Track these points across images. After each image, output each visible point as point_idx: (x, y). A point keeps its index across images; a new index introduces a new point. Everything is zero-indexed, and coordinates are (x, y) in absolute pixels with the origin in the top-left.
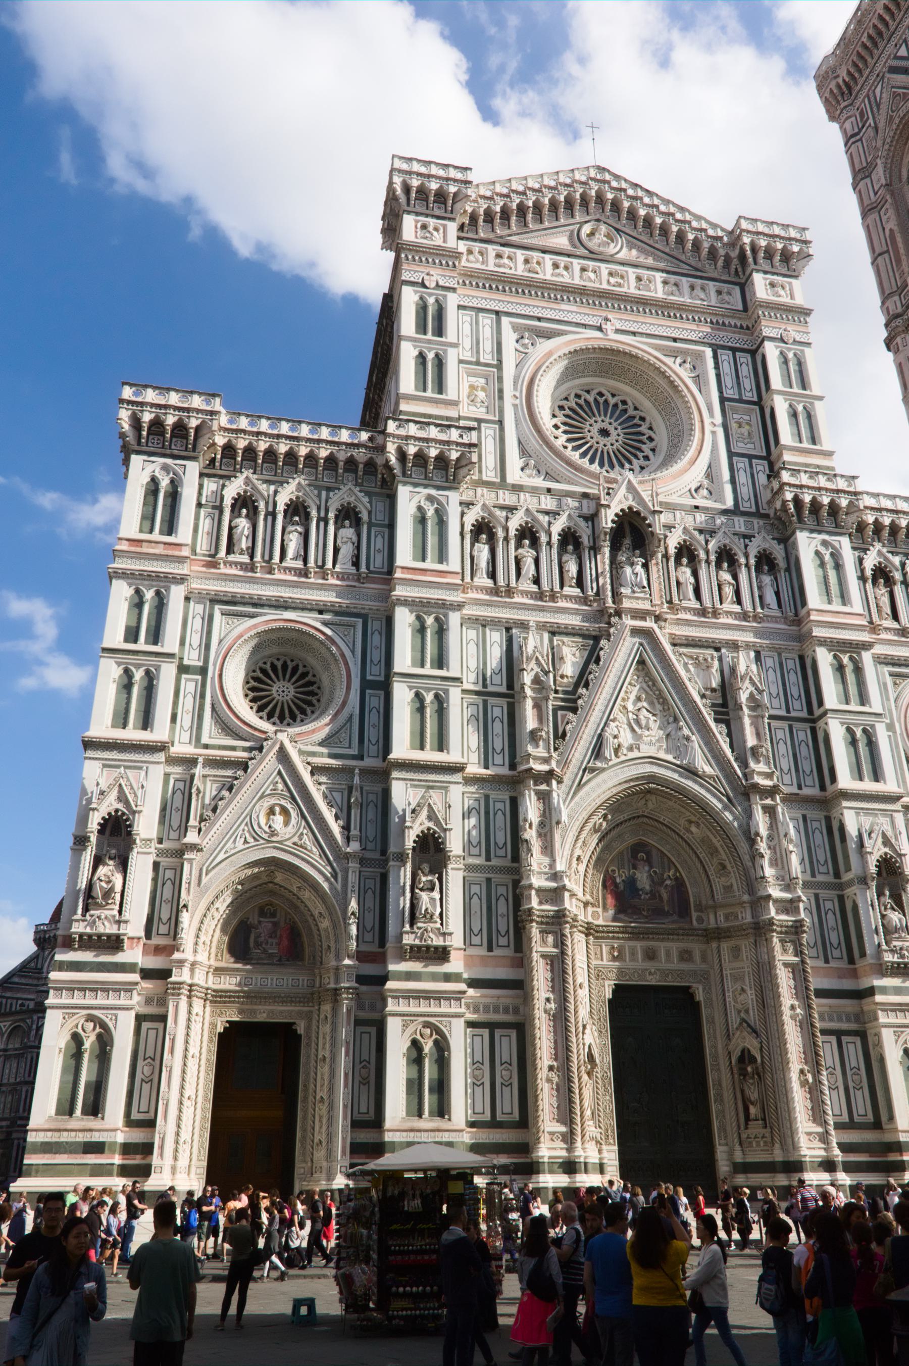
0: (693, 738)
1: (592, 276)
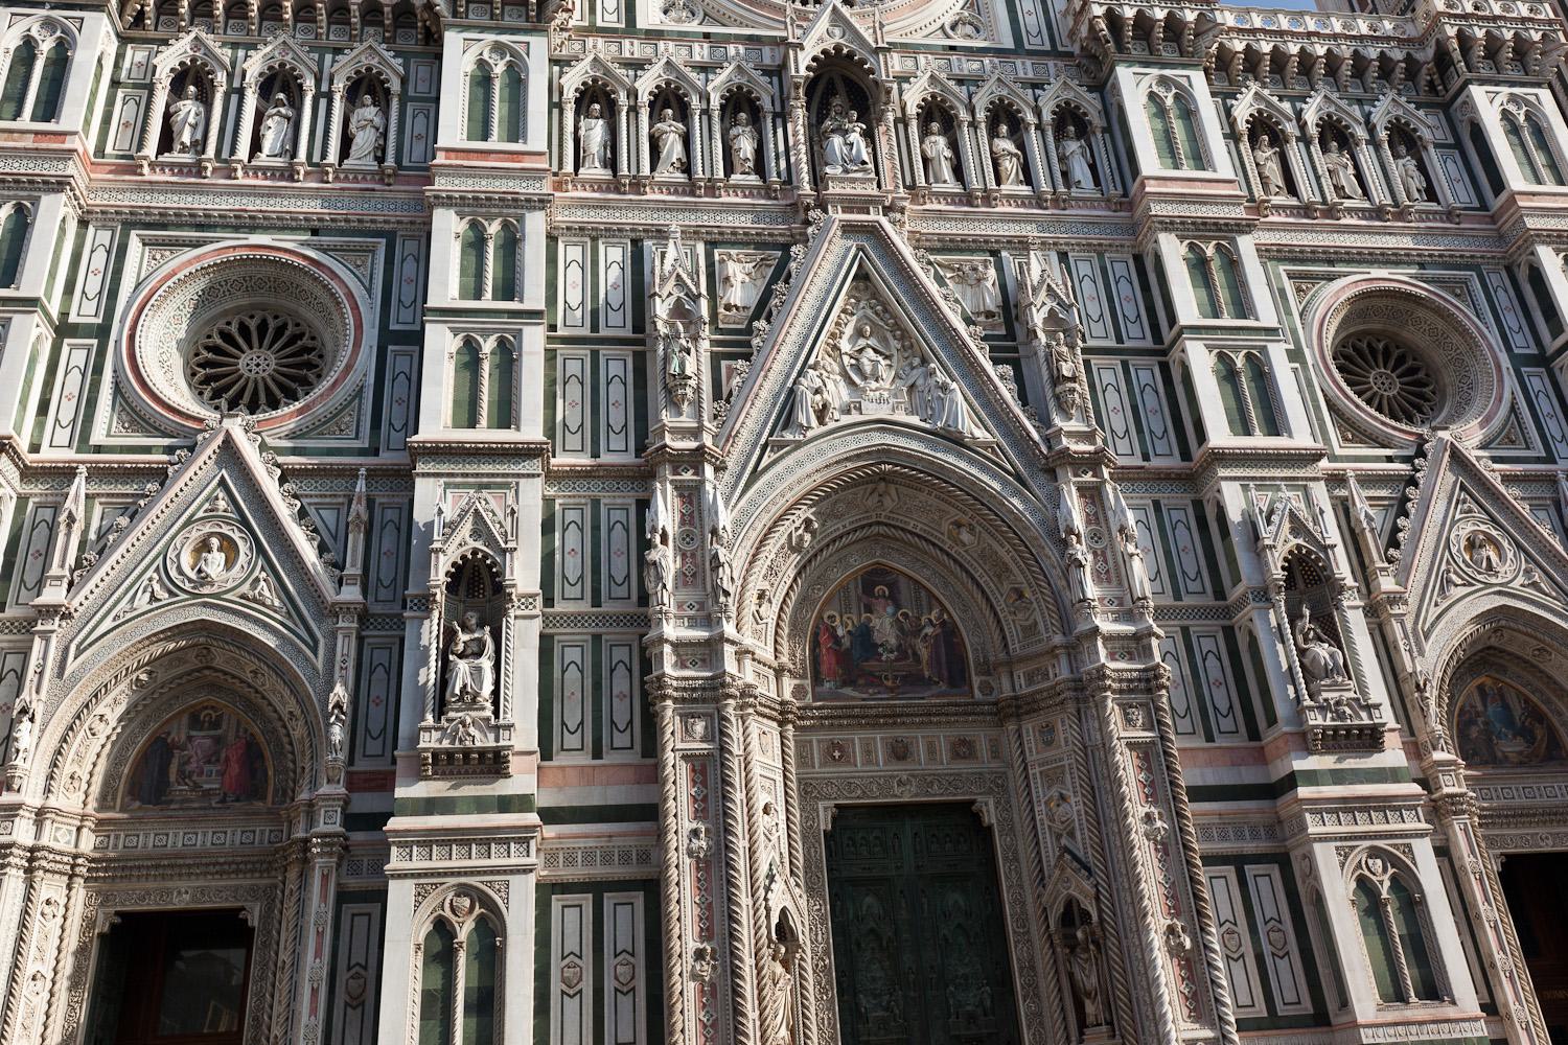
0: (954, 385)
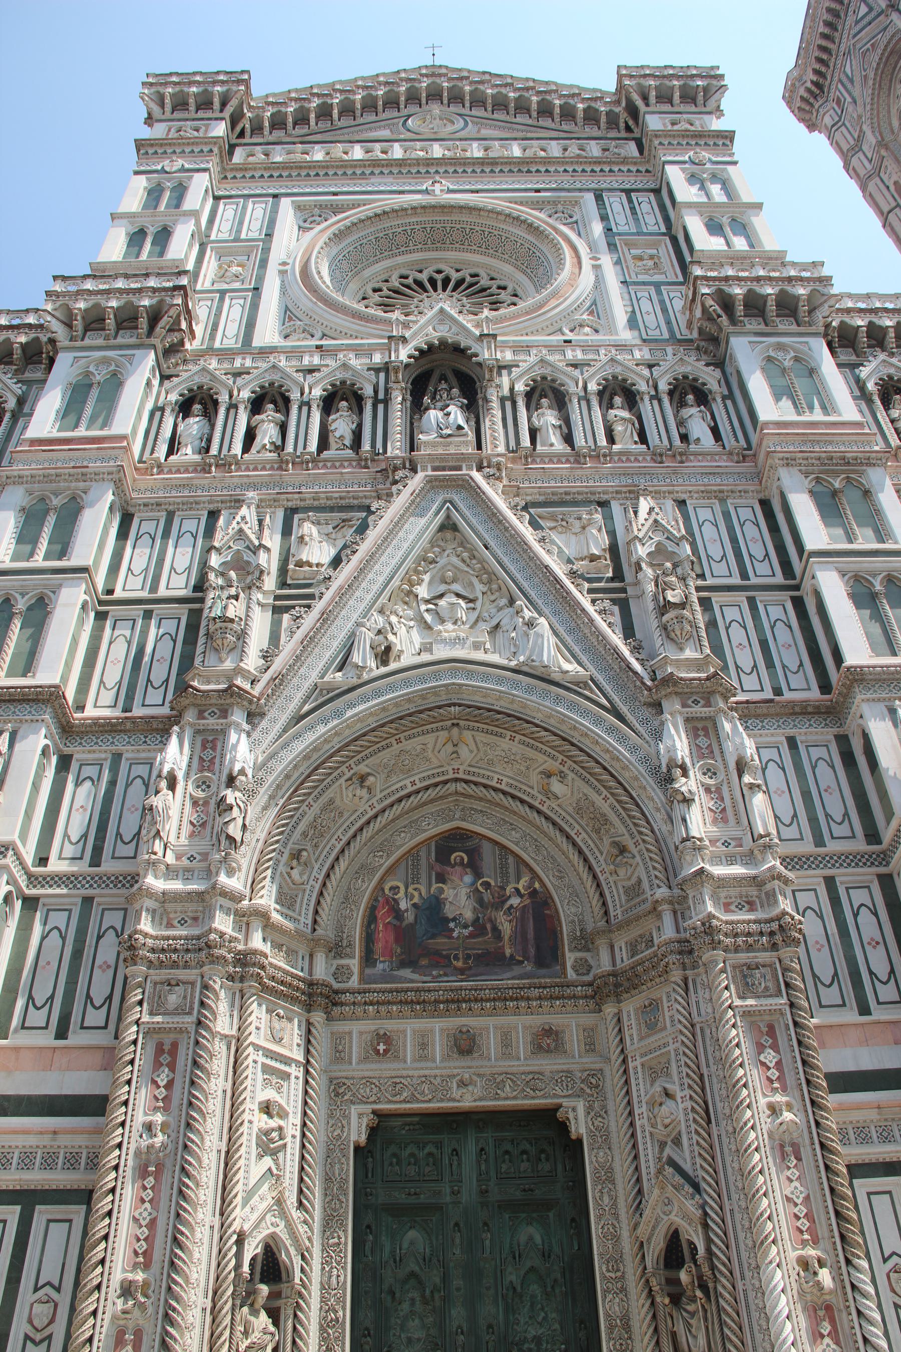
1: (421, 154)
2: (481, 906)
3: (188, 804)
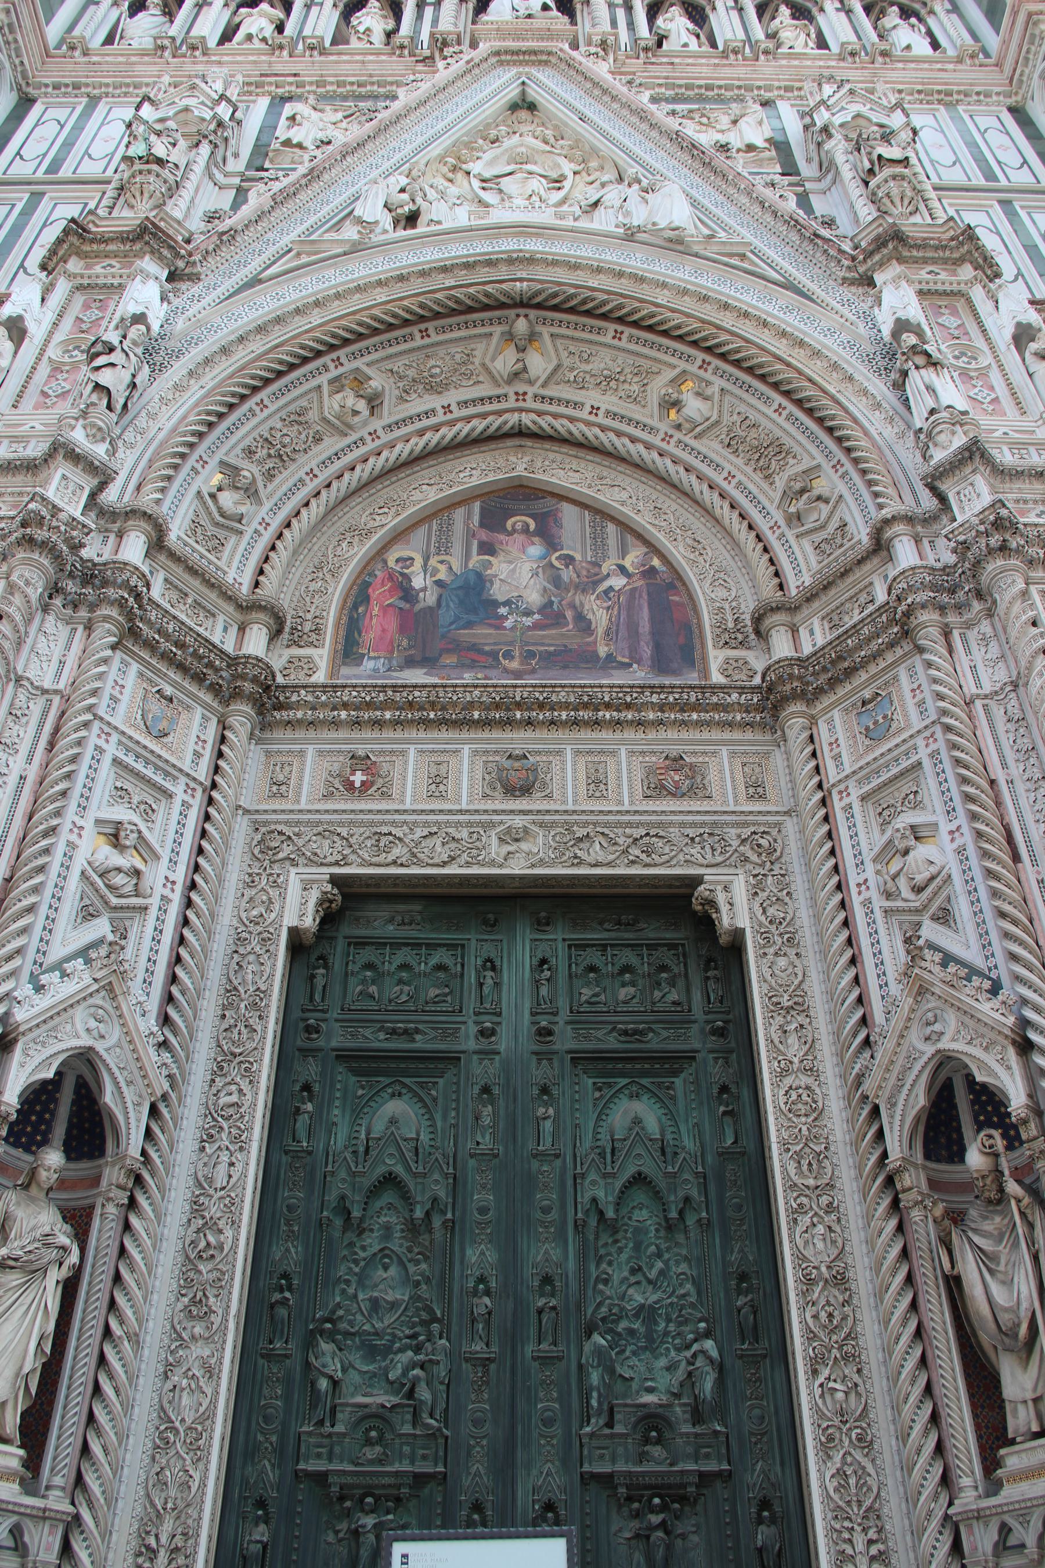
2: (557, 587)
3: (44, 370)
